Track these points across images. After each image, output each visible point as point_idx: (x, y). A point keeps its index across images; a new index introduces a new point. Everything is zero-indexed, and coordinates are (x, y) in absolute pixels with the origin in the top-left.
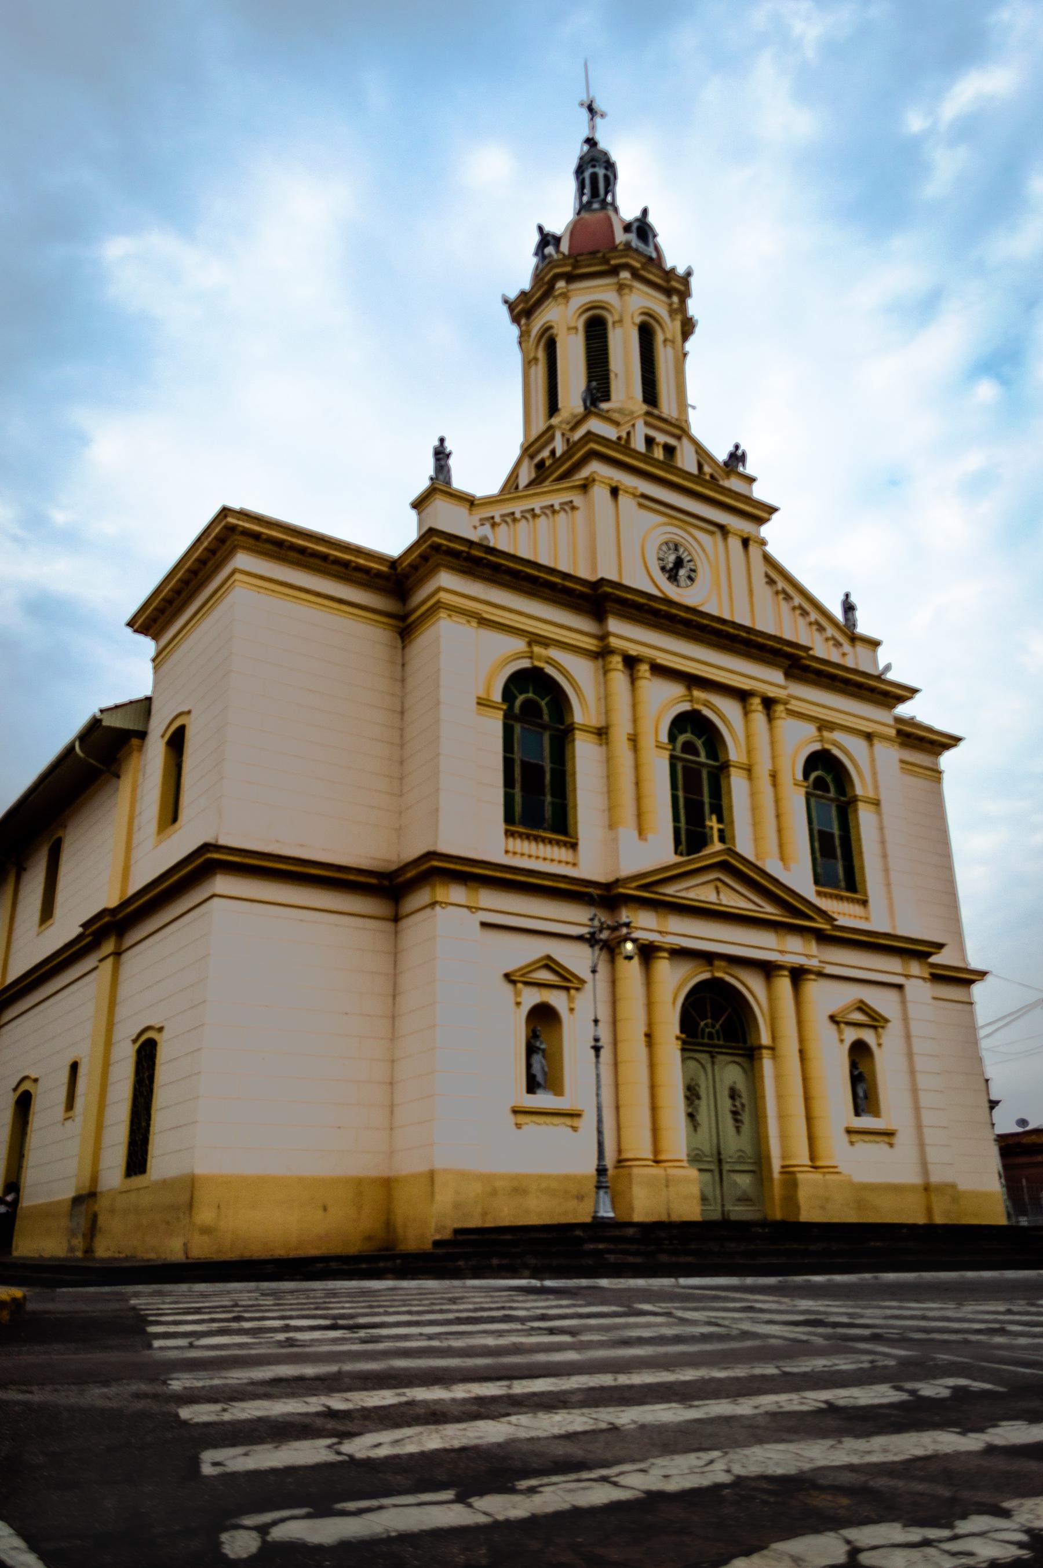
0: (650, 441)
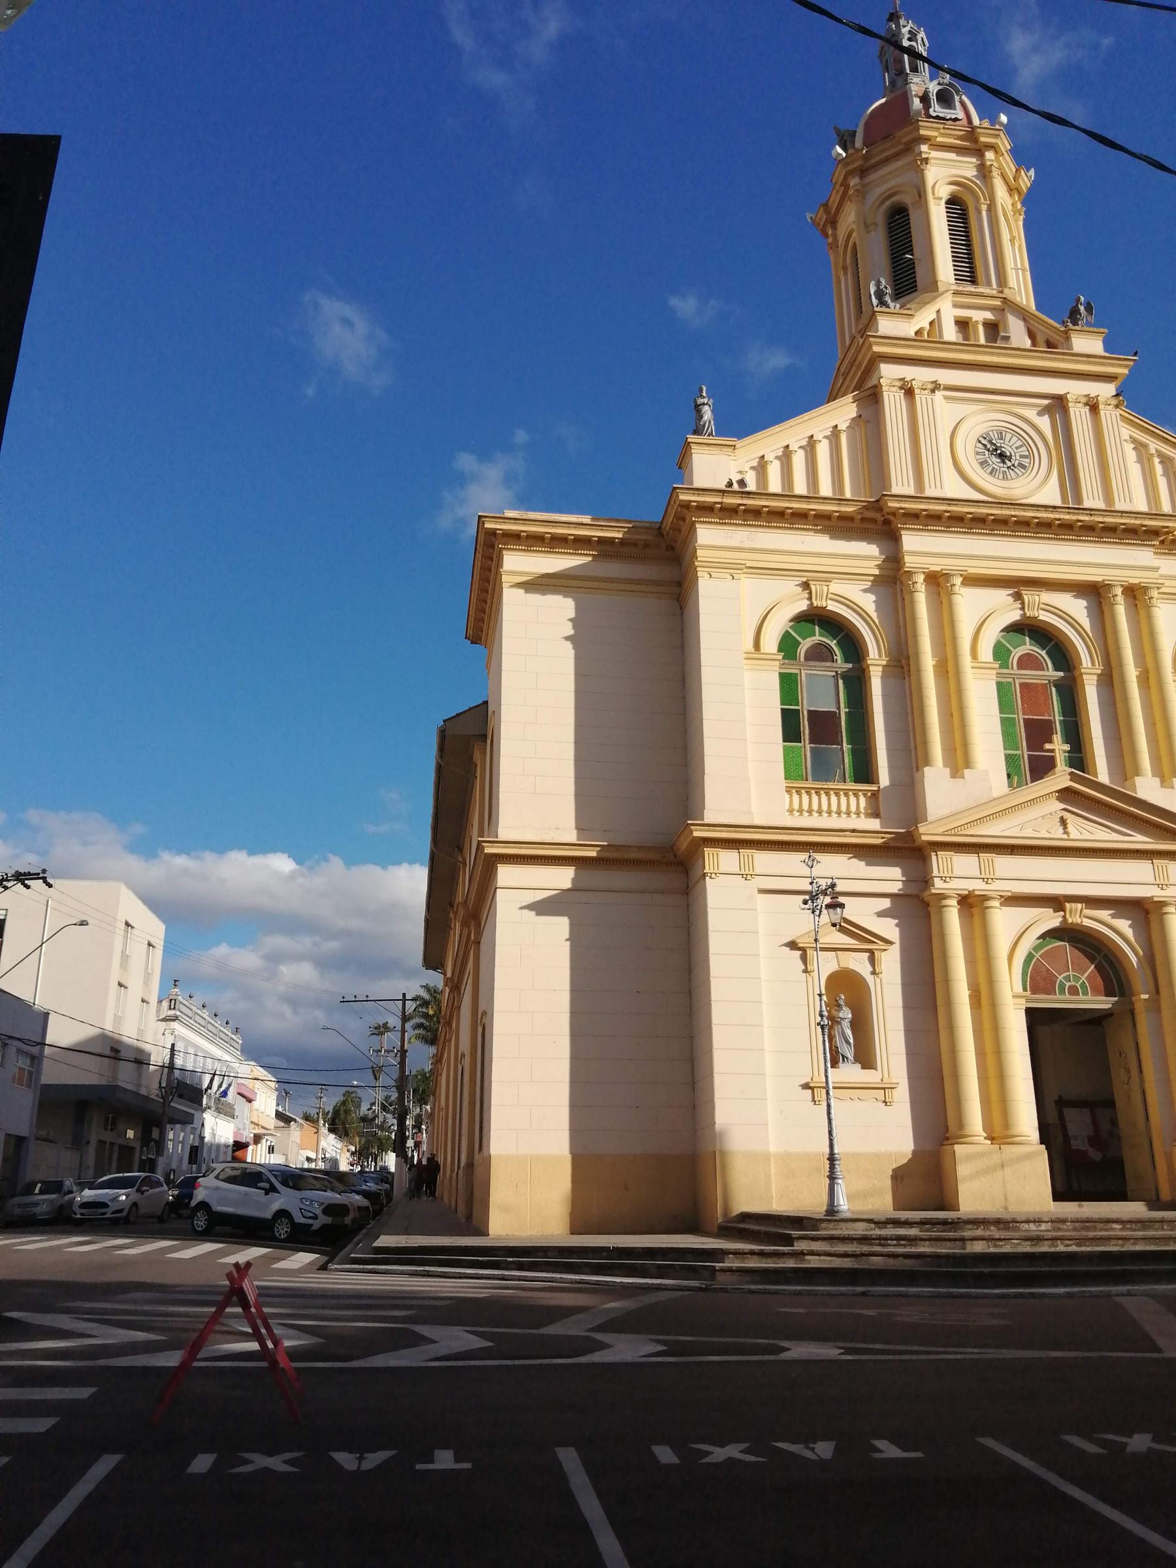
0: (963, 325)
